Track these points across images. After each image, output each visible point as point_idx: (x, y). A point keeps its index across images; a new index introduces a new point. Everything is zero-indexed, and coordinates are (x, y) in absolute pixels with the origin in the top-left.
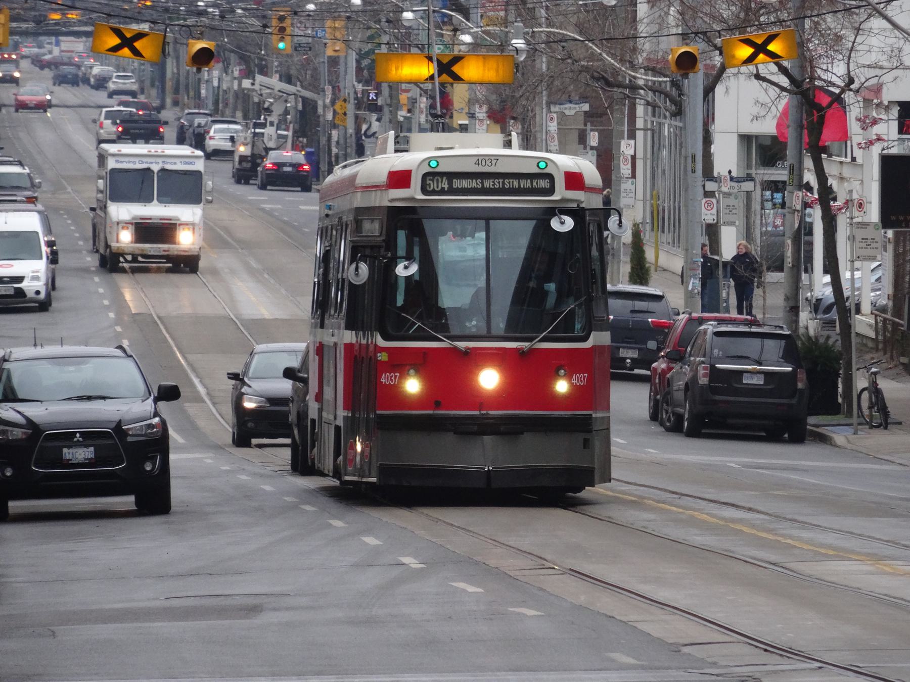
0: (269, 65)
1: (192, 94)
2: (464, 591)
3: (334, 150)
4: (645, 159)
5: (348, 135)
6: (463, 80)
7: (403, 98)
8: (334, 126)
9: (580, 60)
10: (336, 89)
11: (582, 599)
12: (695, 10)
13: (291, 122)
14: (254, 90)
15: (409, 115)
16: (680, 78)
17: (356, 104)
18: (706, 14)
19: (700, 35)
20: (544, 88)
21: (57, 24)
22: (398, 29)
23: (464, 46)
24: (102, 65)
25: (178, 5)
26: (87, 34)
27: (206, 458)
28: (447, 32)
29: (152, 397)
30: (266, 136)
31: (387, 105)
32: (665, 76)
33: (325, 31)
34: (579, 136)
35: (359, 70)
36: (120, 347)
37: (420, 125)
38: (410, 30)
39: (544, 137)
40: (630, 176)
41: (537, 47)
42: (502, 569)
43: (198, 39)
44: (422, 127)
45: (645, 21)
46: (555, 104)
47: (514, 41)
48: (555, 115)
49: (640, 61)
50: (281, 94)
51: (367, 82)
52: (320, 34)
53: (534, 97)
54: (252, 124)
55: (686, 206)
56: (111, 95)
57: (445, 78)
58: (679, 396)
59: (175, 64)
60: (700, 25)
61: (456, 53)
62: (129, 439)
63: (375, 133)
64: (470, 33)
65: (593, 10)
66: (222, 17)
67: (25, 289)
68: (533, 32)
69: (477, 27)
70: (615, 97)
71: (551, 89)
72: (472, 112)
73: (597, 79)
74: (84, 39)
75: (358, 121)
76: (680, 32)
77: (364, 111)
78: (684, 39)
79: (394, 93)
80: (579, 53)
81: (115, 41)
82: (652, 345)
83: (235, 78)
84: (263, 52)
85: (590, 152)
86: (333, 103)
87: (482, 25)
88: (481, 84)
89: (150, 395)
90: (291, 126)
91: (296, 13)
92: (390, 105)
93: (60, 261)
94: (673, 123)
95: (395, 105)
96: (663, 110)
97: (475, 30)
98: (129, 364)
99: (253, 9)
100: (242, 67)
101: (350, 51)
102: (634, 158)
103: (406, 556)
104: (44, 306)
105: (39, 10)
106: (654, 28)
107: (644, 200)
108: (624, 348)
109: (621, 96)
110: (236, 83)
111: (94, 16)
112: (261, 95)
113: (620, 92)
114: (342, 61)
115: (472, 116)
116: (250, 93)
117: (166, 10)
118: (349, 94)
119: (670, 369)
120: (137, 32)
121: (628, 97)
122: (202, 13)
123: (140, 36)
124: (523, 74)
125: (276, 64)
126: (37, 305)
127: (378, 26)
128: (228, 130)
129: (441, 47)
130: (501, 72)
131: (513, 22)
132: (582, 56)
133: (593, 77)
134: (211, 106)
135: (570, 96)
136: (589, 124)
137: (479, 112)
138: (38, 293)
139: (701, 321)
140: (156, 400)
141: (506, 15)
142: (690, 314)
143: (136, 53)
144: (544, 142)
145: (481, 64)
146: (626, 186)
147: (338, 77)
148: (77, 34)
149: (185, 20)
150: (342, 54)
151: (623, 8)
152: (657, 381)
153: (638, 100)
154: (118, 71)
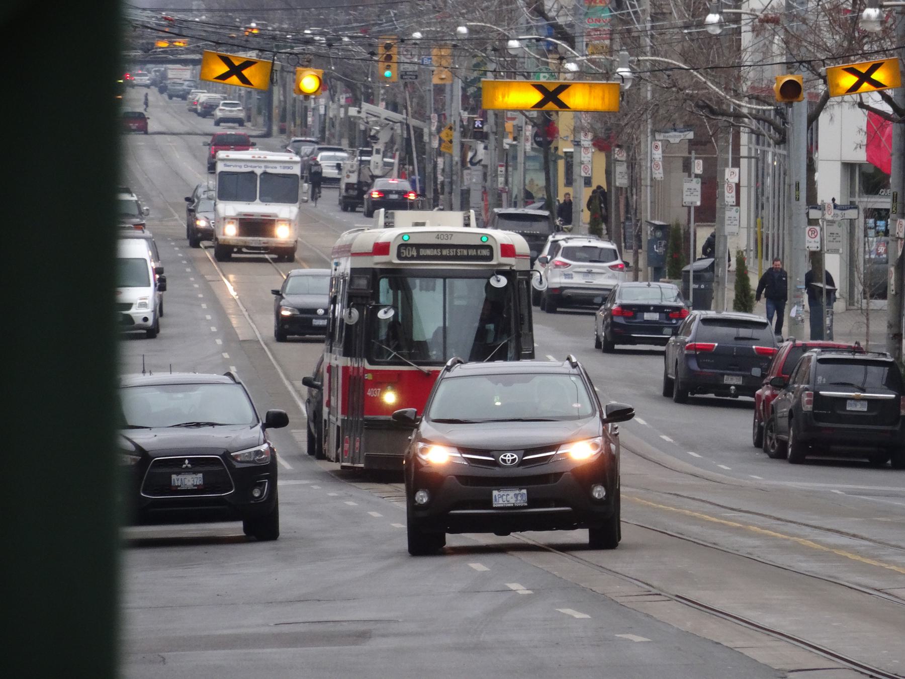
0: (376, 93)
1: (298, 121)
2: (571, 617)
3: (440, 178)
4: (749, 186)
5: (454, 163)
6: (567, 107)
7: (509, 126)
8: (440, 153)
9: (685, 88)
10: (442, 117)
11: (688, 626)
12: (799, 39)
13: (397, 150)
14: (360, 118)
15: (515, 143)
16: (784, 107)
17: (462, 132)
18: (810, 43)
19: (804, 64)
20: (649, 116)
21: (164, 52)
22: (504, 58)
23: (570, 74)
24: (209, 92)
25: (285, 34)
26: (194, 62)
27: (313, 485)
28: (552, 61)
29: (260, 424)
30: (372, 163)
31: (493, 132)
32: (770, 105)
33: (431, 59)
34: (683, 164)
35: (465, 98)
36: (229, 374)
37: (525, 152)
38: (516, 59)
39: (649, 165)
40: (734, 204)
41: (642, 75)
42: (609, 595)
43: (306, 66)
44: (527, 155)
45: (749, 49)
46: (660, 131)
47: (619, 70)
48: (660, 143)
49: (745, 89)
50: (387, 122)
51: (473, 110)
52: (426, 61)
53: (639, 126)
54: (358, 152)
55: (790, 234)
56: (217, 123)
57: (551, 106)
58: (784, 422)
59: (282, 92)
60: (803, 54)
61: (561, 81)
62: (238, 466)
63: (481, 161)
64: (575, 62)
65: (697, 39)
66: (330, 45)
67: (133, 316)
68: (639, 60)
69: (583, 56)
70: (720, 125)
71: (656, 117)
72: (577, 140)
73: (701, 108)
74: (191, 67)
75: (464, 148)
76: (785, 61)
77: (470, 139)
78: (788, 68)
79: (500, 121)
80: (684, 82)
81: (224, 69)
82: (756, 372)
83: (342, 106)
84: (370, 79)
85: (695, 180)
86: (439, 130)
87: (587, 53)
88: (587, 112)
89: (259, 422)
90: (398, 153)
91: (403, 41)
92: (496, 133)
93: (168, 287)
94: (777, 151)
95: (500, 133)
96: (767, 137)
97: (581, 58)
98: (238, 392)
99: (360, 37)
100: (348, 95)
101: (456, 79)
102: (738, 186)
103: (514, 582)
104: (151, 332)
105: (147, 38)
106: (758, 57)
107: (748, 228)
108: (728, 374)
109: (726, 124)
110: (342, 110)
111: (201, 44)
112: (367, 123)
113: (725, 121)
114: (448, 89)
115: (577, 144)
116: (357, 121)
117: (274, 38)
118: (455, 121)
119: (774, 396)
120: (245, 60)
121: (733, 125)
122: (309, 42)
123: (248, 64)
124: (628, 102)
125: (382, 91)
126: (145, 331)
127: (484, 55)
128: (334, 158)
129: (546, 75)
130: (607, 100)
131: (618, 51)
132: (686, 85)
133: (697, 106)
134: (317, 134)
135: (674, 125)
136: (693, 152)
137: (584, 141)
138: (146, 319)
139: (805, 348)
140: (265, 427)
141: (611, 44)
142: (794, 341)
143: (245, 80)
144: (649, 170)
145: (586, 90)
146: (730, 214)
147: (444, 104)
148: (185, 62)
149: (292, 48)
150: (448, 83)
151: (728, 37)
152: (761, 407)
153: (742, 128)
154: (225, 99)
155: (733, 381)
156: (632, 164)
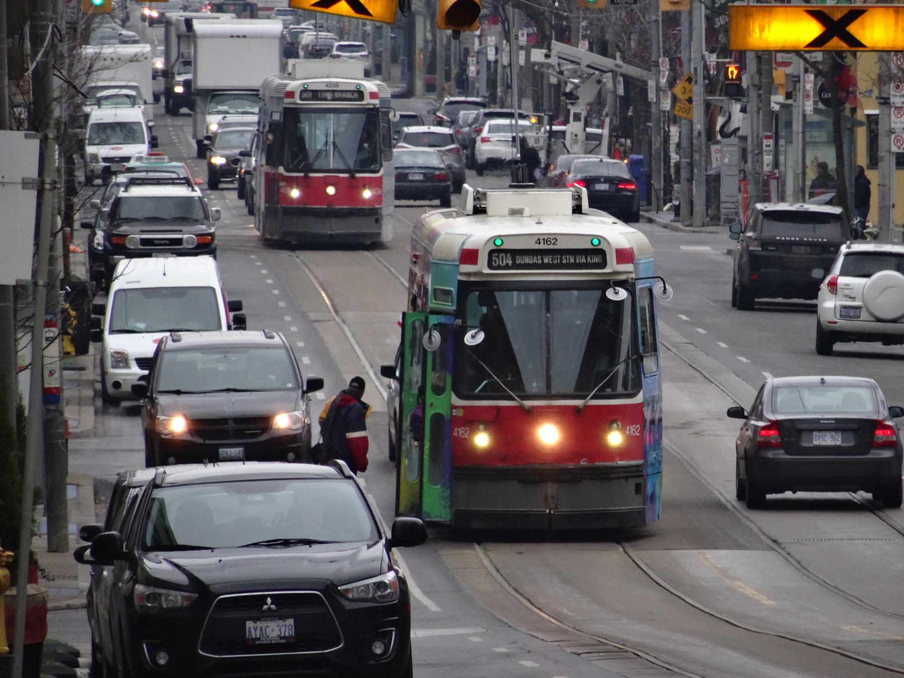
3: (674, 157)
8: (675, 120)
134: (484, 90)
140: (389, 546)
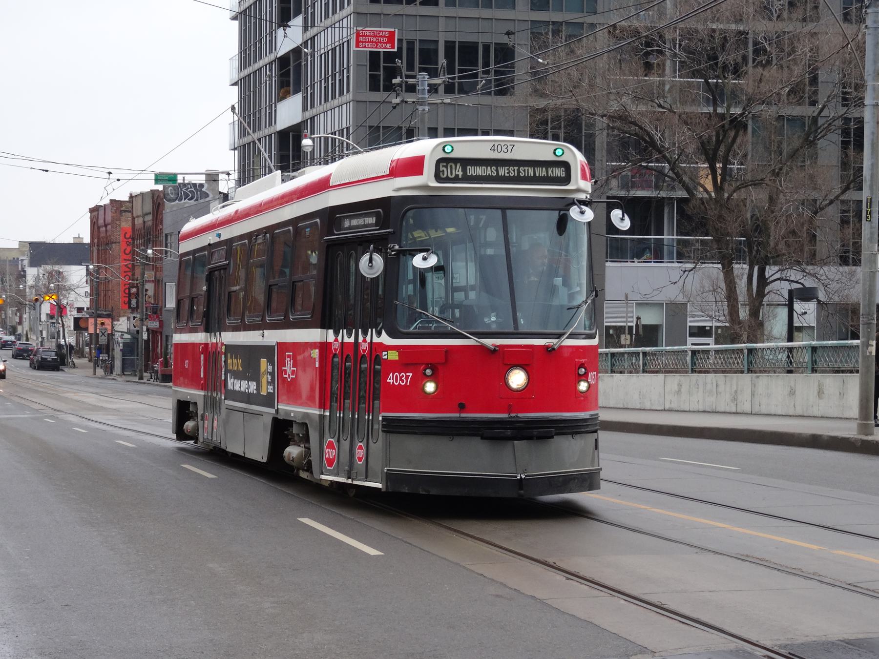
155: (25, 355)
156: (5, 314)
